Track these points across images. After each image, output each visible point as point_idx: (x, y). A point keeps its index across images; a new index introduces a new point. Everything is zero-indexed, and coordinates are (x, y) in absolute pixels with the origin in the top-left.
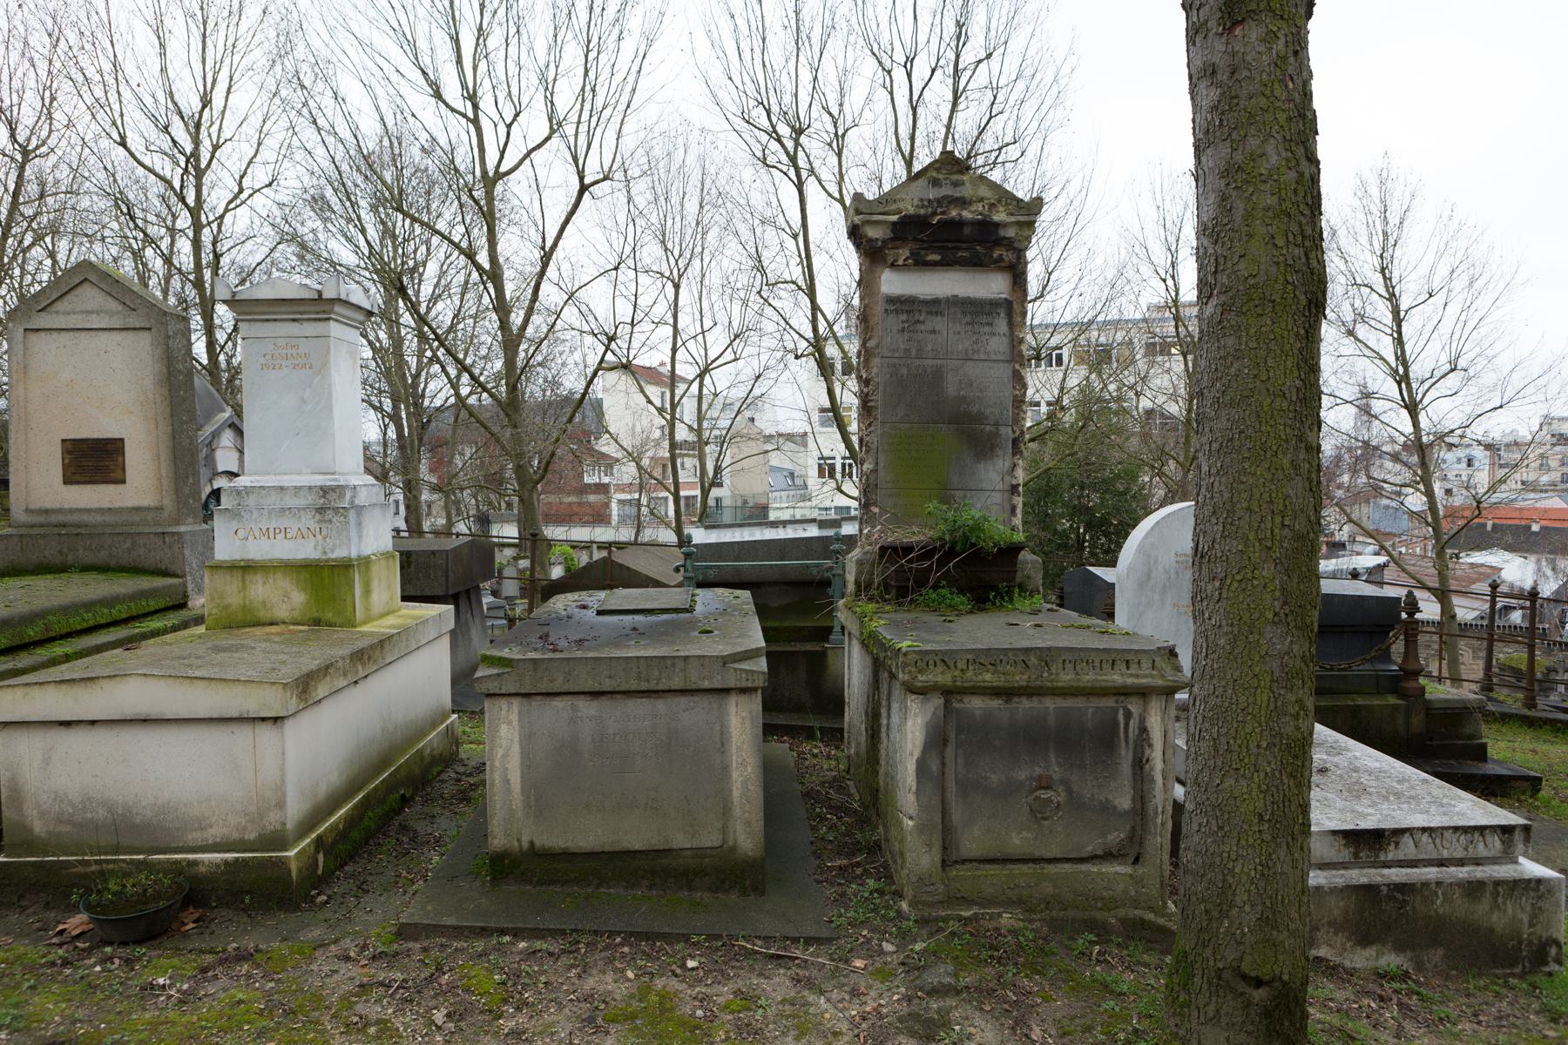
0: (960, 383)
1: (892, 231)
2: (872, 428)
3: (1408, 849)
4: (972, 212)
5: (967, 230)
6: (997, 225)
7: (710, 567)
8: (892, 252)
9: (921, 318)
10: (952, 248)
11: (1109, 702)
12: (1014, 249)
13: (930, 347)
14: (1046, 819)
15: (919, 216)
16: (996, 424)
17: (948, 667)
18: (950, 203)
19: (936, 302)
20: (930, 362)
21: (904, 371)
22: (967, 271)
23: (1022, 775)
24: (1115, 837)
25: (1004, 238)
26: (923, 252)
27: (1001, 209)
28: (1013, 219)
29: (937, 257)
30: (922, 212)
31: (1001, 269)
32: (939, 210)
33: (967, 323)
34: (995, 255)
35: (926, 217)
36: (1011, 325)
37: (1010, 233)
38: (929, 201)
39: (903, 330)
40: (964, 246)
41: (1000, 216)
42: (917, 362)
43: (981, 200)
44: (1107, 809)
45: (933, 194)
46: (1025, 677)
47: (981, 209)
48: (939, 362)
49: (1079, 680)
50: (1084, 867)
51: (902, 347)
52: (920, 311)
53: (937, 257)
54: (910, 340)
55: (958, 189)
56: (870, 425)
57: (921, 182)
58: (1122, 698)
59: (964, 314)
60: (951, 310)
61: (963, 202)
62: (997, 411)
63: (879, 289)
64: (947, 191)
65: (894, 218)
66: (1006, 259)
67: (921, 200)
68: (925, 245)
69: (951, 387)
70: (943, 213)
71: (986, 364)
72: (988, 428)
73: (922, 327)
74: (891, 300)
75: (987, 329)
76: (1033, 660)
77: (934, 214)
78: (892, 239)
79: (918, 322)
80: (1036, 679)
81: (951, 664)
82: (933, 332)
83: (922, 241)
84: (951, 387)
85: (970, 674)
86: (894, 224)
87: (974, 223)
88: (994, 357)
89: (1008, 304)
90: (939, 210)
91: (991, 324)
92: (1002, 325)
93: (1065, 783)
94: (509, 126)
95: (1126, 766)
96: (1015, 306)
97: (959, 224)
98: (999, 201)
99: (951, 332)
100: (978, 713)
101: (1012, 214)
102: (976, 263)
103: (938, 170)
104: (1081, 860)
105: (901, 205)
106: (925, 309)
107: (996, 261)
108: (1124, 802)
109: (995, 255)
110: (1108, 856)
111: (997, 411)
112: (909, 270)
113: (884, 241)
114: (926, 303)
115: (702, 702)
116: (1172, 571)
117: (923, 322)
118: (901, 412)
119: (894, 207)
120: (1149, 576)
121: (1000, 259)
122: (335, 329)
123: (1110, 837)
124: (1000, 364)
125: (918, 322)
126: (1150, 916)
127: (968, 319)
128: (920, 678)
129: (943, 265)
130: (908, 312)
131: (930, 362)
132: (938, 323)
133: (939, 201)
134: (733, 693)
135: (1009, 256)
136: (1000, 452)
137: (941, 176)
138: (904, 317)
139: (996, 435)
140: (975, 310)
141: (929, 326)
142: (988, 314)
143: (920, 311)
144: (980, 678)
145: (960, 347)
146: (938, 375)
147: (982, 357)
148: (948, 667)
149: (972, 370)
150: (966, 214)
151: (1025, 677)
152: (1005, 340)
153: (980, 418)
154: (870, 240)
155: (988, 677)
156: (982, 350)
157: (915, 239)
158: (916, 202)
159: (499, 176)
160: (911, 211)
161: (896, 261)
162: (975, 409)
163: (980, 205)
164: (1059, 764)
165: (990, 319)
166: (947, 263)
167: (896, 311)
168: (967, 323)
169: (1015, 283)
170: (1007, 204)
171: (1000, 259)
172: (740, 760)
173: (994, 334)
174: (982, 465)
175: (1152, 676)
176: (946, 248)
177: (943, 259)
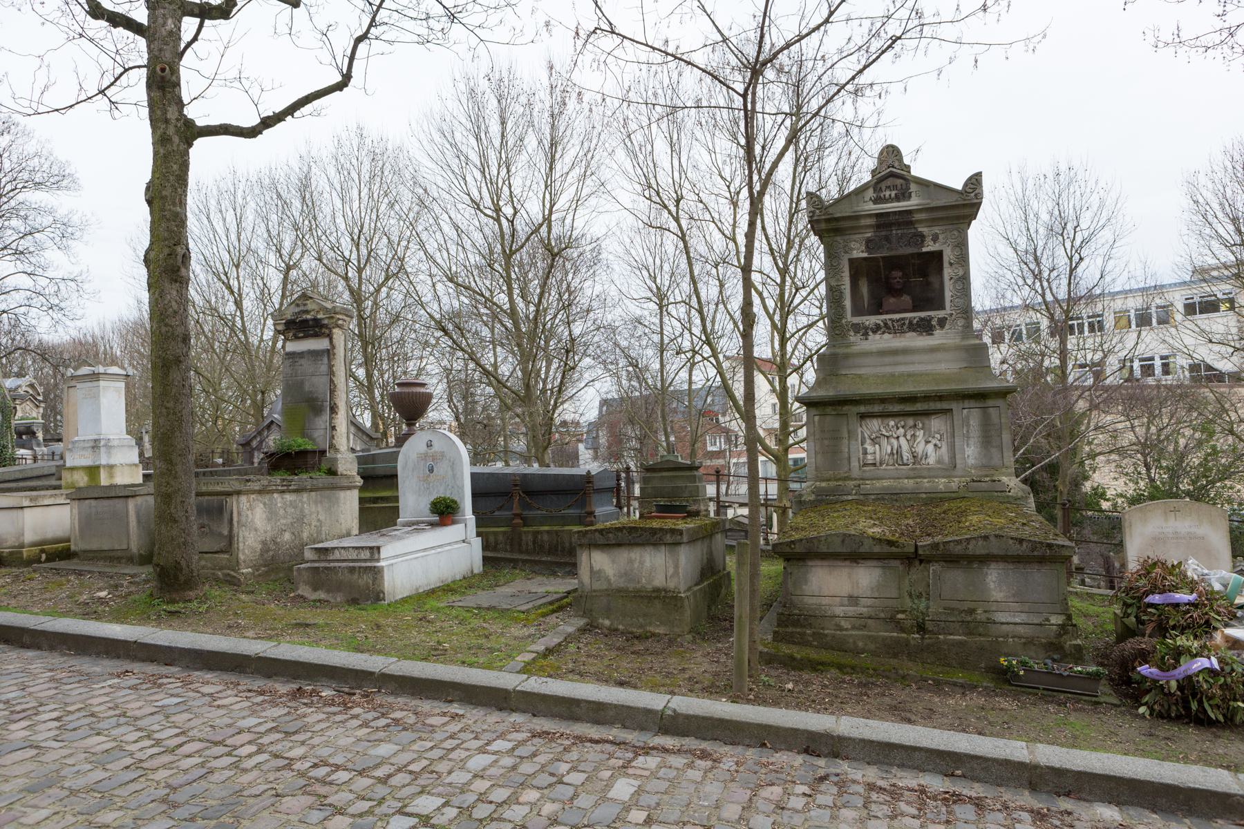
3: (337, 555)
5: (311, 323)
6: (321, 319)
19: (303, 353)
24: (223, 544)
29: (302, 335)
36: (329, 360)
37: (326, 322)
41: (320, 316)
44: (220, 535)
45: (297, 310)
50: (217, 555)
53: (302, 335)
57: (293, 306)
61: (307, 312)
64: (302, 308)
69: (307, 388)
84: (307, 388)
89: (328, 350)
92: (325, 360)
93: (208, 525)
94: (512, 222)
95: (226, 520)
97: (306, 321)
102: (316, 335)
108: (226, 532)
110: (221, 552)
114: (299, 354)
115: (122, 500)
120: (406, 463)
122: (102, 383)
126: (232, 573)
132: (302, 361)
135: (327, 331)
139: (322, 406)
140: (315, 354)
146: (302, 383)
149: (315, 380)
150: (309, 317)
153: (316, 399)
159: (513, 253)
162: (315, 395)
166: (306, 337)
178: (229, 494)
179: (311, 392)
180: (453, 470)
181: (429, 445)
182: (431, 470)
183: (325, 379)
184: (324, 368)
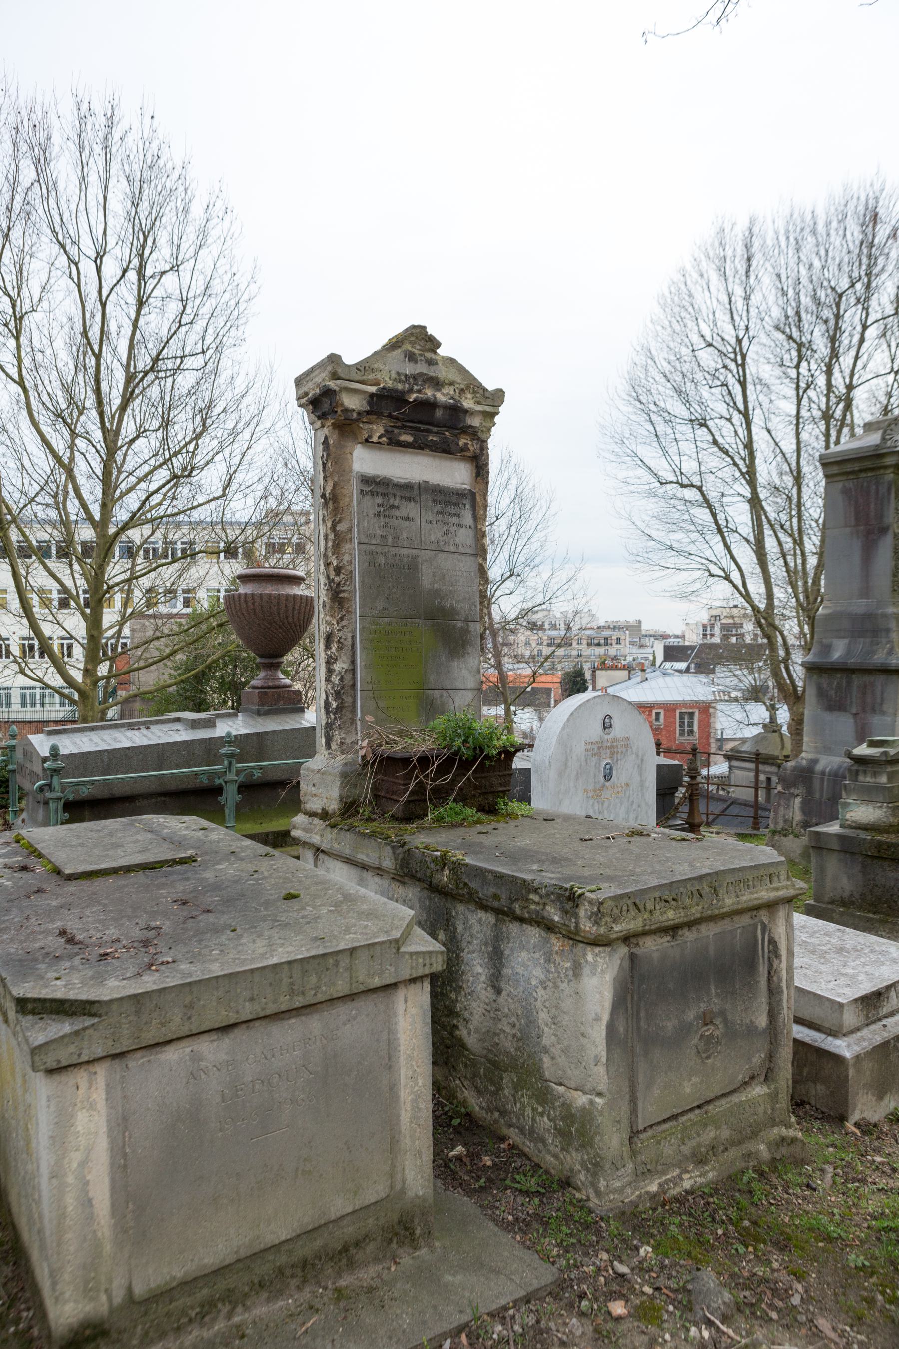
0: (434, 576)
1: (369, 403)
2: (344, 623)
4: (444, 395)
5: (439, 413)
6: (466, 411)
7: (84, 784)
8: (366, 426)
9: (396, 503)
10: (423, 431)
11: (745, 920)
12: (479, 439)
13: (405, 535)
14: (708, 1057)
15: (396, 391)
16: (466, 620)
17: (639, 910)
18: (424, 381)
19: (408, 486)
20: (405, 551)
21: (381, 560)
22: (434, 456)
23: (690, 1015)
25: (471, 426)
26: (396, 431)
27: (469, 396)
28: (479, 408)
30: (400, 387)
31: (464, 458)
32: (415, 387)
33: (438, 512)
34: (462, 442)
35: (403, 393)
36: (475, 517)
37: (476, 422)
38: (406, 375)
39: (378, 515)
40: (435, 429)
41: (468, 403)
42: (393, 550)
43: (452, 384)
44: (751, 1030)
45: (409, 369)
46: (699, 908)
47: (452, 392)
48: (414, 552)
49: (738, 903)
50: (735, 1099)
51: (379, 532)
52: (394, 495)
54: (385, 526)
55: (432, 368)
56: (342, 619)
57: (397, 353)
58: (754, 913)
59: (434, 501)
60: (423, 497)
61: (437, 383)
62: (467, 607)
63: (350, 466)
64: (421, 368)
65: (373, 389)
66: (472, 449)
67: (398, 374)
68: (399, 424)
70: (419, 391)
71: (457, 555)
72: (460, 624)
73: (397, 513)
74: (366, 480)
75: (455, 520)
76: (706, 890)
77: (411, 391)
78: (368, 413)
79: (393, 506)
80: (708, 909)
81: (641, 907)
82: (407, 519)
83: (397, 418)
84: (426, 579)
85: (657, 913)
86: (372, 395)
87: (446, 407)
88: (462, 550)
89: (473, 494)
90: (415, 387)
91: (459, 515)
92: (467, 517)
96: (478, 498)
97: (430, 405)
98: (468, 387)
99: (423, 520)
100: (656, 956)
101: (479, 403)
102: (445, 449)
103: (413, 344)
104: (734, 1091)
105: (379, 376)
106: (398, 494)
107: (462, 450)
108: (762, 1021)
109: (462, 442)
111: (467, 607)
112: (380, 449)
113: (359, 413)
115: (366, 1006)
116: (583, 758)
117: (398, 507)
118: (380, 604)
119: (371, 377)
121: (465, 448)
123: (754, 1060)
124: (468, 558)
125: (393, 506)
127: (438, 507)
128: (616, 928)
129: (414, 448)
130: (384, 495)
131: (405, 551)
132: (410, 509)
133: (415, 377)
134: (402, 986)
135: (473, 447)
136: (470, 649)
137: (417, 352)
138: (379, 500)
141: (403, 512)
142: (456, 504)
143: (394, 495)
144: (665, 917)
145: (433, 538)
146: (413, 566)
147: (452, 549)
148: (639, 910)
149: (446, 562)
150: (441, 397)
151: (699, 908)
152: (471, 533)
154: (346, 410)
155: (671, 914)
156: (452, 542)
157: (390, 416)
158: (394, 375)
160: (390, 384)
161: (370, 436)
163: (452, 388)
164: (717, 995)
165: (457, 510)
166: (418, 446)
167: (372, 493)
168: (438, 512)
169: (478, 474)
170: (474, 392)
171: (465, 448)
172: (410, 1073)
173: (461, 525)
174: (456, 663)
175: (786, 887)
176: (418, 429)
177: (415, 441)
178: (771, 906)
179: (436, 593)
180: (641, 775)
181: (607, 726)
182: (608, 777)
183: (467, 565)
184: (465, 537)
